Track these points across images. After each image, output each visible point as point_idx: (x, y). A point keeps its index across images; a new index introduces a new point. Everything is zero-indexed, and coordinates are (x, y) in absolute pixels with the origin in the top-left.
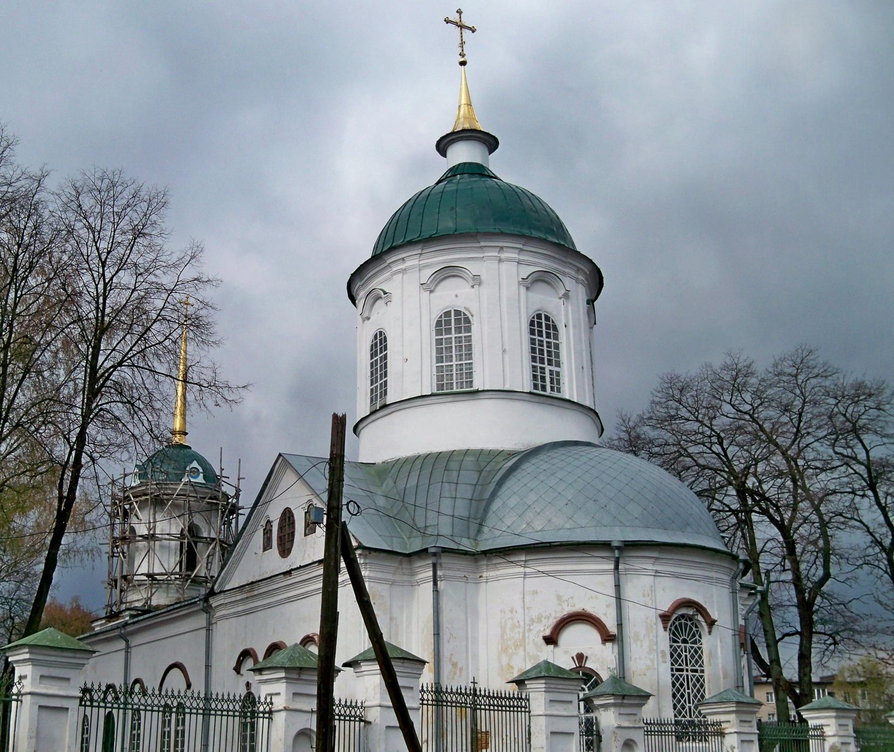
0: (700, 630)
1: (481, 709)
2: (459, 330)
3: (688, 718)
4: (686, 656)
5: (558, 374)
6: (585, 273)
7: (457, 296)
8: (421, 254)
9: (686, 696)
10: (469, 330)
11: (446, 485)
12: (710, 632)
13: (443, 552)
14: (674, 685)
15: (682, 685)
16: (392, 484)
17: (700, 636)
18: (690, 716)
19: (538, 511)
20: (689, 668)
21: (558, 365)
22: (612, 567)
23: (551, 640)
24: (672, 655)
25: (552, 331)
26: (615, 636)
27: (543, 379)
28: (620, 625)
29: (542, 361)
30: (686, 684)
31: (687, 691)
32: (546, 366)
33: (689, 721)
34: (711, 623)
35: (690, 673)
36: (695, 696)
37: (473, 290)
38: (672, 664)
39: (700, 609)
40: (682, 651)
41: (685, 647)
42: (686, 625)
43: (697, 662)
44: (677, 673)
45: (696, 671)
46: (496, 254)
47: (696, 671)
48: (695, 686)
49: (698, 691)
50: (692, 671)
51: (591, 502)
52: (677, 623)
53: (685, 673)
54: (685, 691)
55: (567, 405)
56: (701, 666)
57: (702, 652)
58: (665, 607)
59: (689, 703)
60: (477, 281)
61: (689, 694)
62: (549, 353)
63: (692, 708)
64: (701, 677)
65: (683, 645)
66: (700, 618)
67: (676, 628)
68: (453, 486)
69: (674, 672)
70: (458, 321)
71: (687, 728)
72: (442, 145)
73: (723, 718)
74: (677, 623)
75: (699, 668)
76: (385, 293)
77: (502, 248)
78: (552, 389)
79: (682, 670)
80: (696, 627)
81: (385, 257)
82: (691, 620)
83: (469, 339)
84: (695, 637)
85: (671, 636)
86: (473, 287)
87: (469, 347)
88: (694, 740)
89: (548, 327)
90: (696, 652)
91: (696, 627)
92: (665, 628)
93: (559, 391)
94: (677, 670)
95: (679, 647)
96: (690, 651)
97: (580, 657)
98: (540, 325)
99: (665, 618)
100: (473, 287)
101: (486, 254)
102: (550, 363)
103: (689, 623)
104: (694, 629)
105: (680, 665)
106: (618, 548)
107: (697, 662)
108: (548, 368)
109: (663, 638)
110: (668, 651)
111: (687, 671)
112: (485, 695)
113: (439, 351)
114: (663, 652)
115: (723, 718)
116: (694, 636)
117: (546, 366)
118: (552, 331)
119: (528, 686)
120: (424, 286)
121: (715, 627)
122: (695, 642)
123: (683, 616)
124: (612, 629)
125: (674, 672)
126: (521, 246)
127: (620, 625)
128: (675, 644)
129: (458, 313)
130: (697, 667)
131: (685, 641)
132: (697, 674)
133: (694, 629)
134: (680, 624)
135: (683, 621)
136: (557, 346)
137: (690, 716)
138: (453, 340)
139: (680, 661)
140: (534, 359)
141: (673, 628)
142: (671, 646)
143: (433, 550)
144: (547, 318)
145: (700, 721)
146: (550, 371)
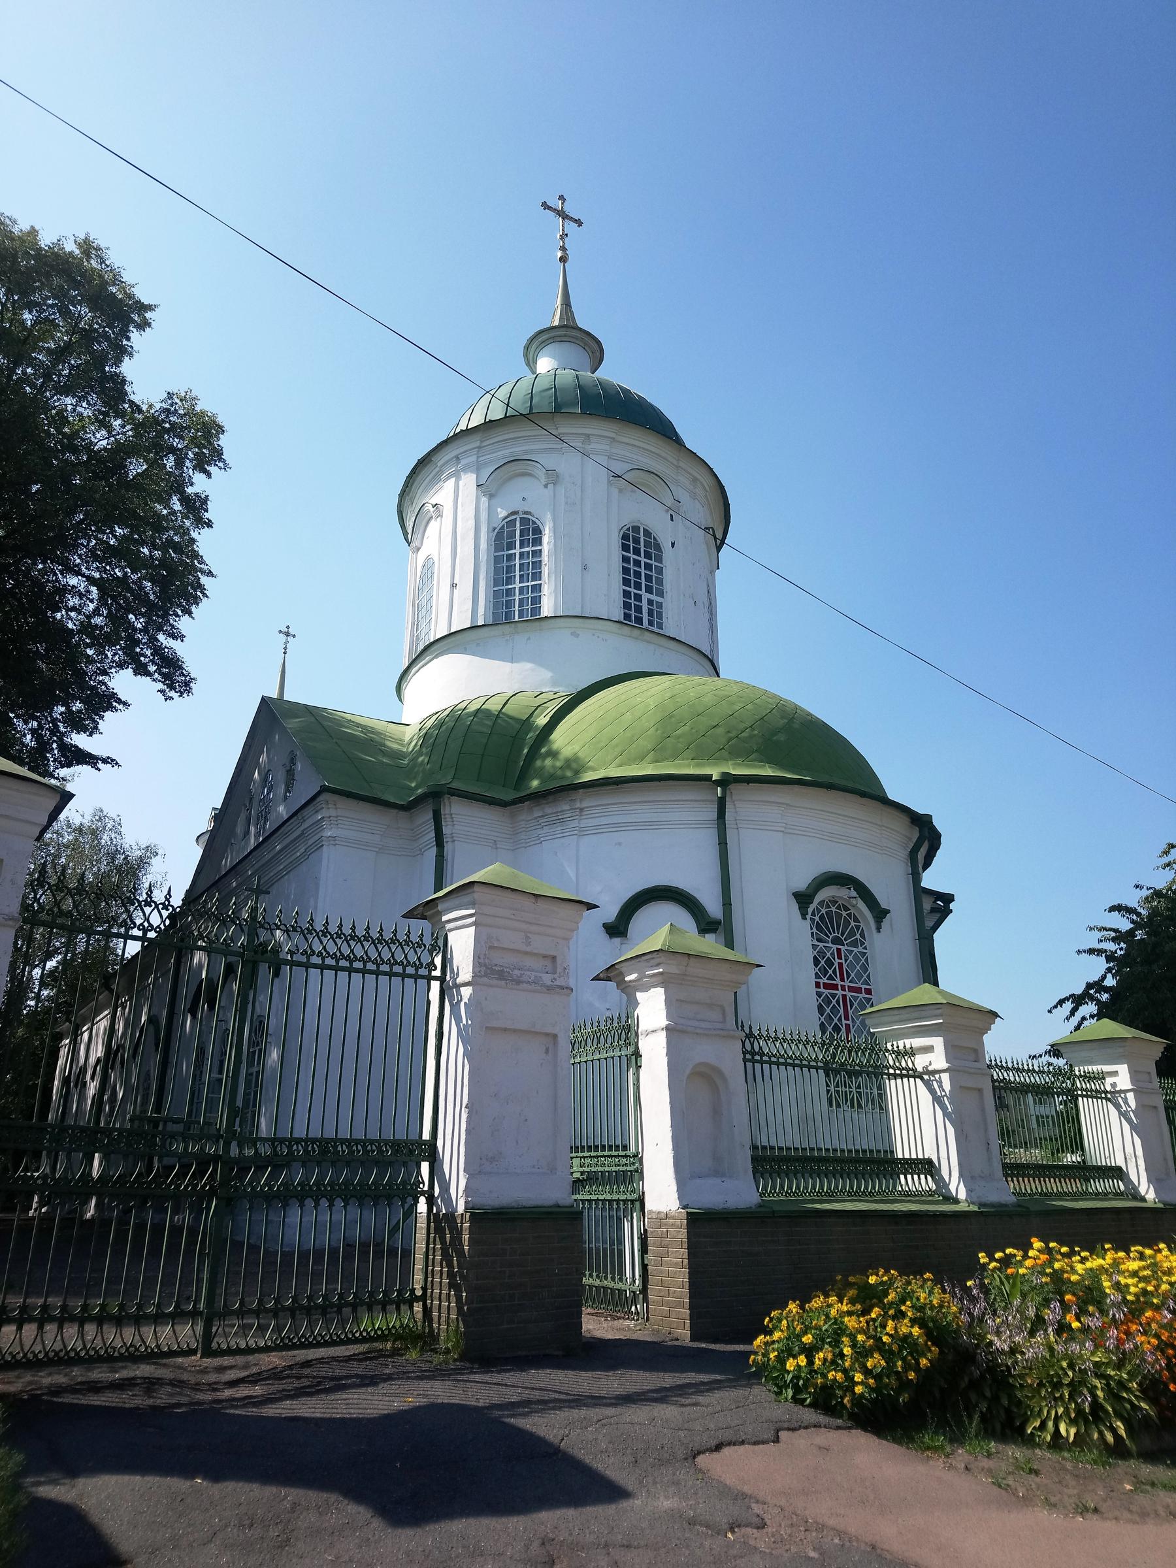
0: (862, 925)
4: (840, 965)
5: (660, 605)
6: (705, 489)
7: (524, 499)
8: (479, 447)
12: (879, 929)
14: (821, 1010)
20: (847, 984)
21: (661, 593)
25: (653, 551)
26: (719, 923)
27: (639, 609)
29: (638, 586)
31: (844, 1022)
32: (643, 592)
34: (880, 914)
37: (545, 490)
38: (817, 975)
40: (832, 954)
41: (839, 950)
43: (859, 976)
44: (827, 991)
45: (859, 990)
47: (859, 990)
53: (840, 992)
55: (673, 644)
57: (867, 960)
58: (802, 884)
60: (553, 477)
62: (649, 578)
65: (835, 947)
66: (861, 905)
67: (822, 917)
69: (822, 990)
75: (863, 987)
77: (588, 436)
78: (651, 623)
79: (835, 987)
85: (815, 930)
86: (546, 486)
87: (537, 565)
89: (647, 544)
91: (856, 920)
92: (804, 917)
93: (660, 626)
94: (826, 986)
98: (637, 541)
99: (803, 899)
100: (546, 486)
102: (649, 590)
104: (853, 923)
105: (831, 978)
107: (859, 976)
108: (645, 596)
110: (809, 955)
111: (843, 988)
113: (497, 571)
116: (852, 933)
117: (643, 592)
118: (653, 551)
120: (482, 488)
121: (885, 923)
122: (855, 944)
124: (714, 908)
125: (822, 990)
126: (613, 435)
127: (727, 903)
128: (821, 945)
131: (836, 941)
133: (853, 923)
136: (660, 571)
139: (830, 972)
140: (626, 582)
141: (817, 918)
144: (647, 533)
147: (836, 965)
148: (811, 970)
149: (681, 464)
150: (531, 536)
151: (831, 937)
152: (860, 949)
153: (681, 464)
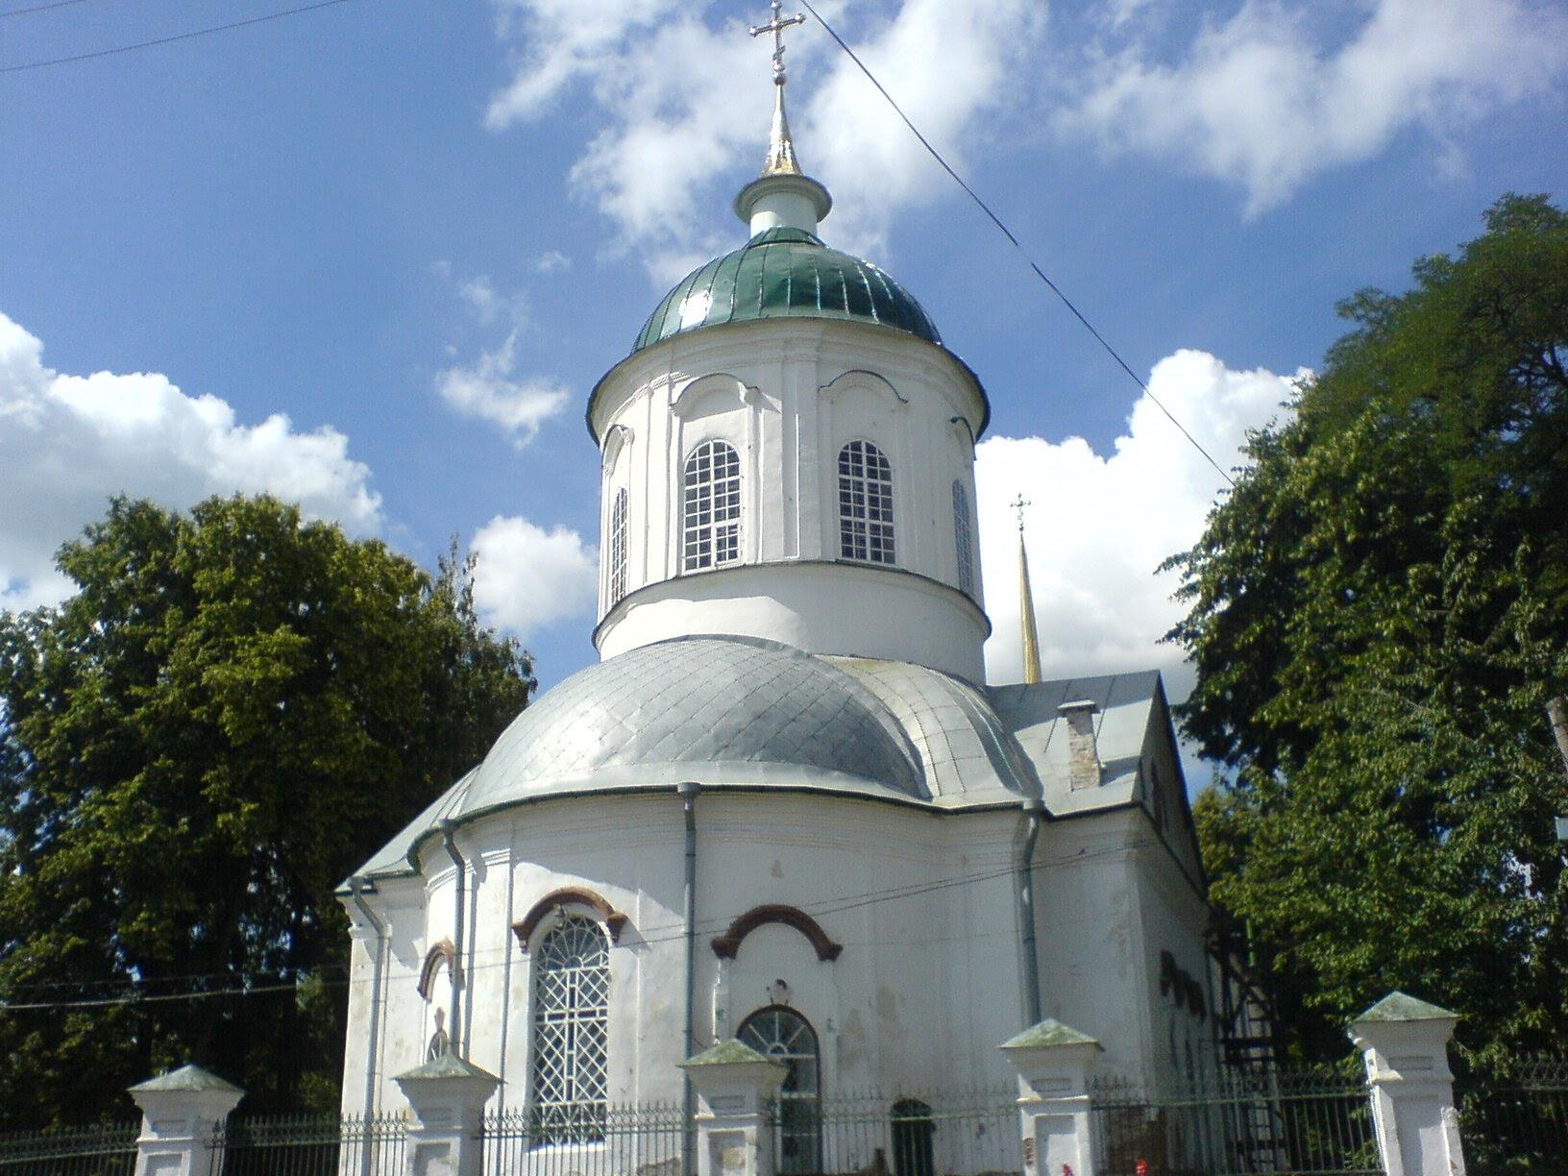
3: (564, 1101)
4: (572, 991)
9: (565, 1061)
30: (565, 1041)
31: (574, 1052)
33: (564, 1108)
34: (618, 924)
35: (577, 1020)
41: (573, 975)
45: (592, 1014)
47: (592, 1014)
48: (584, 1041)
53: (566, 1021)
54: (562, 1053)
59: (570, 1073)
61: (570, 1058)
63: (574, 1083)
64: (601, 1023)
71: (562, 1120)
75: (598, 1009)
78: (720, 557)
88: (574, 1141)
93: (733, 555)
96: (581, 979)
111: (572, 1015)
122: (595, 962)
130: (593, 1007)
137: (569, 1098)
144: (719, 447)
145: (591, 1107)
146: (719, 530)
151: (570, 957)
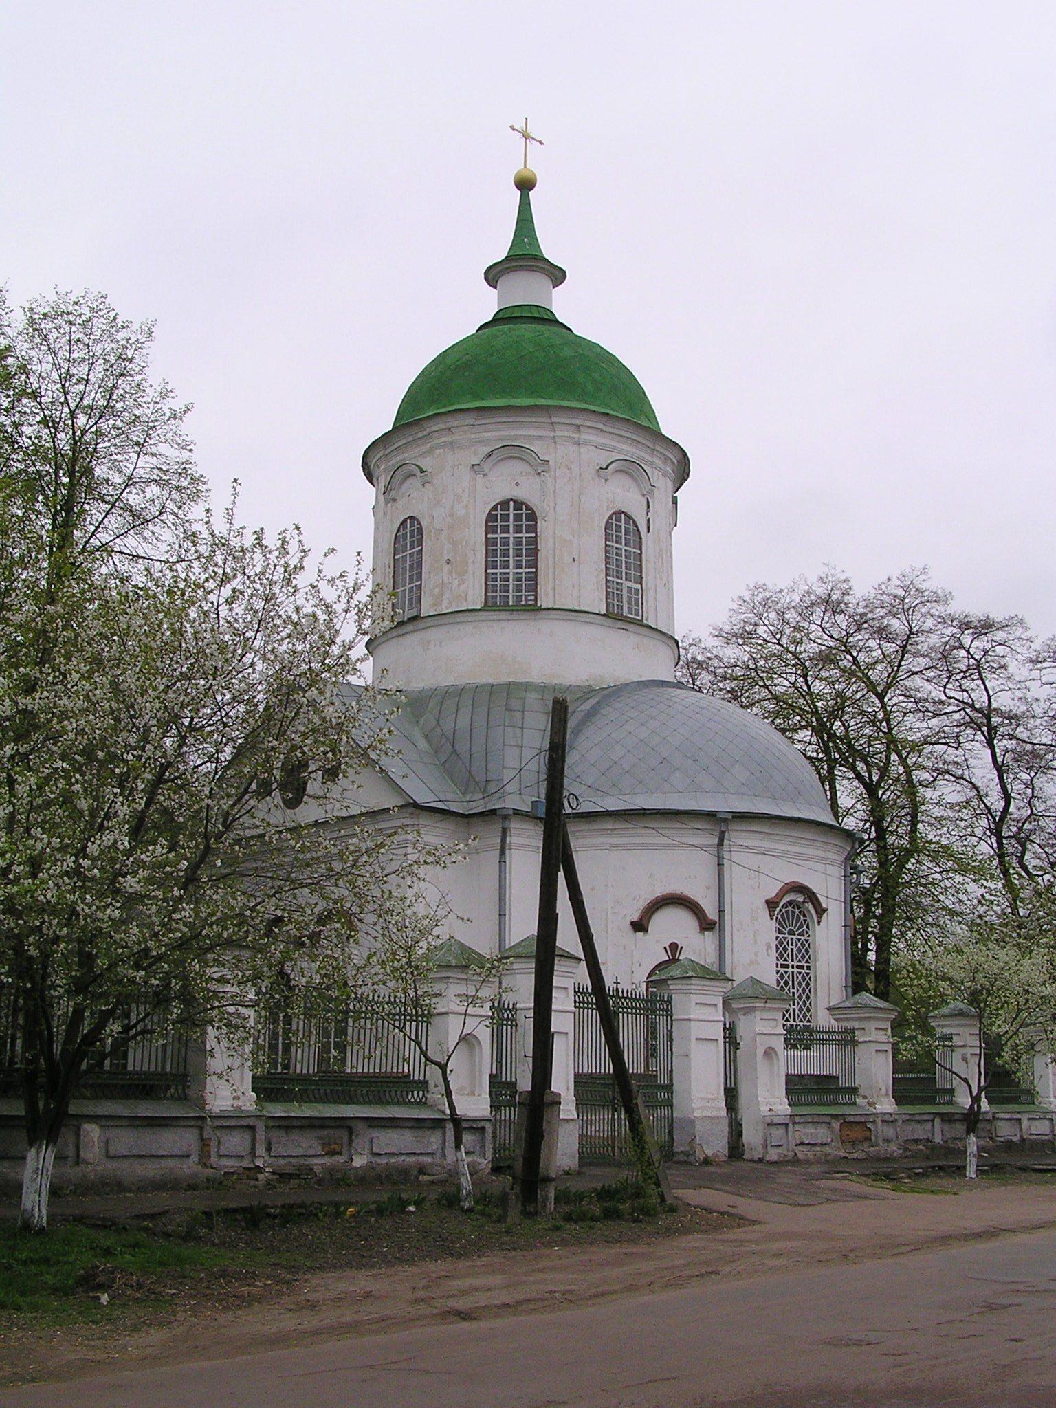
1: (623, 1013)
2: (518, 529)
4: (792, 950)
6: (673, 463)
10: (533, 528)
11: (510, 729)
12: (819, 923)
13: (514, 814)
15: (786, 983)
16: (435, 723)
17: (808, 927)
18: (794, 1021)
19: (627, 769)
22: (716, 841)
23: (639, 926)
24: (777, 949)
27: (620, 597)
28: (721, 911)
34: (821, 911)
35: (796, 970)
36: (800, 997)
39: (811, 896)
42: (794, 913)
43: (803, 957)
44: (782, 970)
45: (802, 967)
46: (569, 434)
47: (802, 967)
48: (800, 984)
49: (804, 991)
50: (798, 967)
51: (690, 761)
52: (784, 910)
53: (790, 970)
56: (807, 962)
58: (772, 894)
63: (797, 1011)
64: (808, 974)
65: (790, 937)
67: (782, 916)
68: (518, 731)
70: (518, 517)
72: (491, 276)
73: (856, 1025)
74: (784, 910)
76: (422, 472)
79: (787, 966)
80: (804, 916)
81: (426, 424)
82: (799, 908)
83: (534, 541)
84: (803, 928)
90: (803, 945)
92: (771, 917)
94: (782, 966)
95: (785, 939)
97: (674, 947)
98: (618, 527)
99: (771, 904)
101: (558, 433)
103: (797, 911)
104: (802, 918)
105: (785, 960)
106: (725, 820)
107: (803, 957)
108: (626, 584)
109: (768, 928)
110: (774, 943)
112: (623, 997)
114: (769, 946)
115: (856, 1025)
116: (801, 926)
119: (671, 987)
122: (801, 934)
123: (790, 903)
124: (711, 913)
126: (601, 426)
128: (781, 936)
129: (519, 505)
130: (803, 963)
131: (791, 932)
132: (803, 971)
133: (802, 918)
134: (787, 912)
135: (790, 908)
137: (794, 1021)
138: (511, 539)
142: (777, 938)
143: (505, 812)
144: (628, 517)
147: (790, 951)
148: (774, 954)
149: (658, 448)
150: (524, 523)
152: (806, 937)
153: (658, 448)
